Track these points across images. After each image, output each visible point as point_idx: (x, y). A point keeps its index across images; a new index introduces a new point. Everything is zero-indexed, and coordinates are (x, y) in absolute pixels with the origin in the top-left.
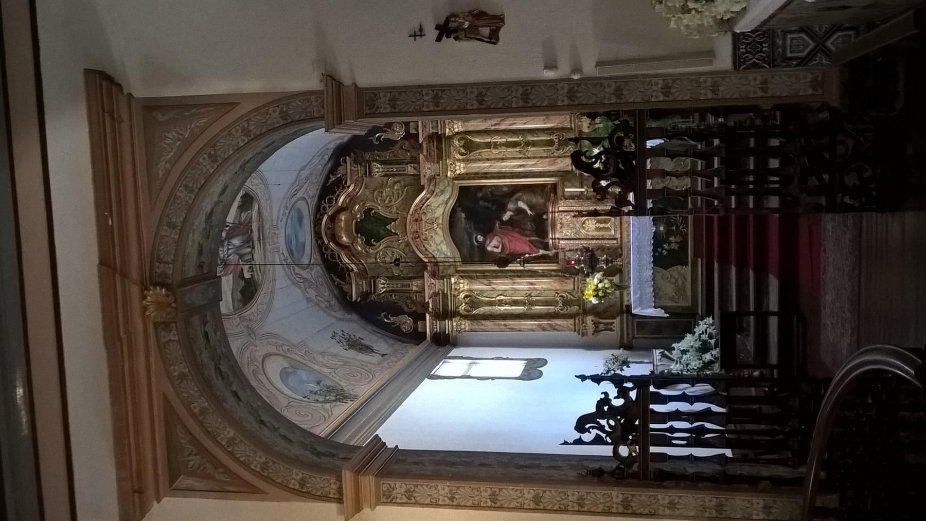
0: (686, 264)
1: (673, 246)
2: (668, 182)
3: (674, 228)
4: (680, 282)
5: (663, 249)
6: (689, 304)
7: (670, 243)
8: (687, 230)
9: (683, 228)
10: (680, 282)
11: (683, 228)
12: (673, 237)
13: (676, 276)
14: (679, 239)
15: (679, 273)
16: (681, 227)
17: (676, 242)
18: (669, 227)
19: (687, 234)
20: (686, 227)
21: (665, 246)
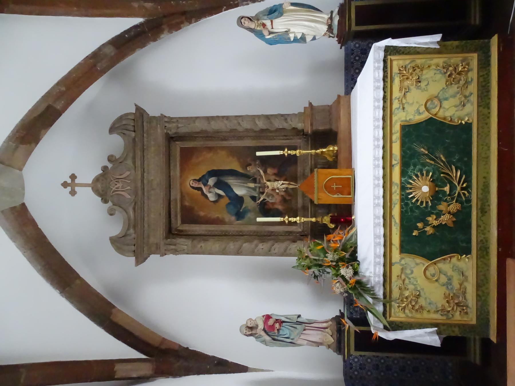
0: (467, 251)
1: (445, 219)
2: (437, 109)
3: (447, 189)
4: (456, 284)
5: (426, 224)
6: (472, 319)
7: (439, 215)
8: (470, 193)
9: (462, 189)
10: (456, 284)
11: (462, 189)
12: (445, 204)
13: (450, 273)
14: (454, 207)
15: (455, 268)
16: (459, 188)
17: (449, 213)
18: (437, 186)
19: (469, 201)
20: (468, 188)
21: (431, 219)
